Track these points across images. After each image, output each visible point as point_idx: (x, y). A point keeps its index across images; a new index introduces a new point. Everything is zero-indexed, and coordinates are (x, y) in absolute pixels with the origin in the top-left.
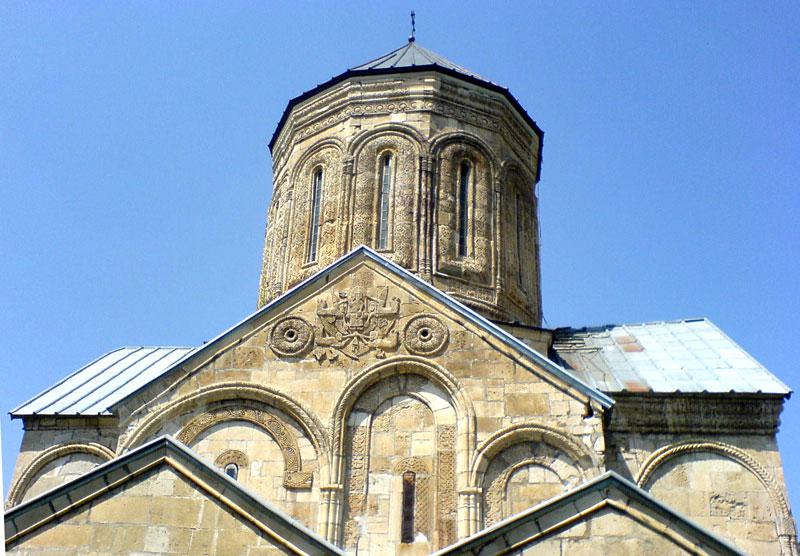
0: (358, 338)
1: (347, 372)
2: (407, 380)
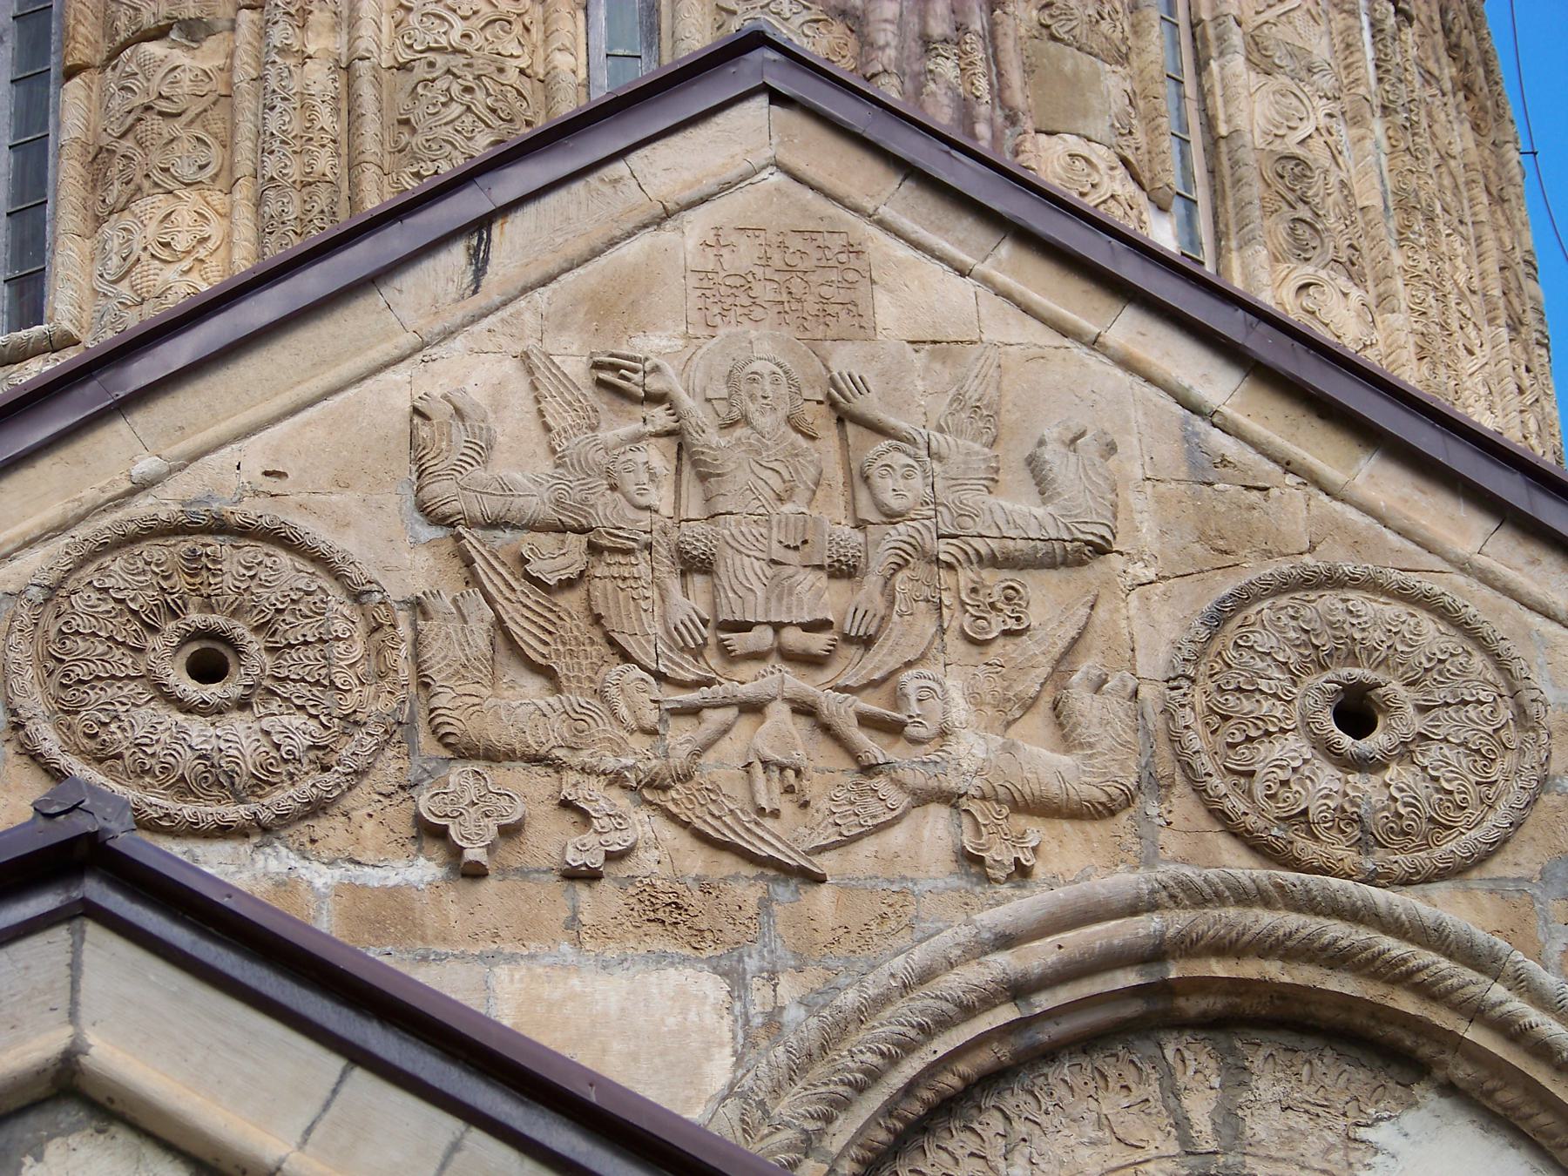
0: (804, 709)
1: (736, 979)
2: (1237, 1075)
